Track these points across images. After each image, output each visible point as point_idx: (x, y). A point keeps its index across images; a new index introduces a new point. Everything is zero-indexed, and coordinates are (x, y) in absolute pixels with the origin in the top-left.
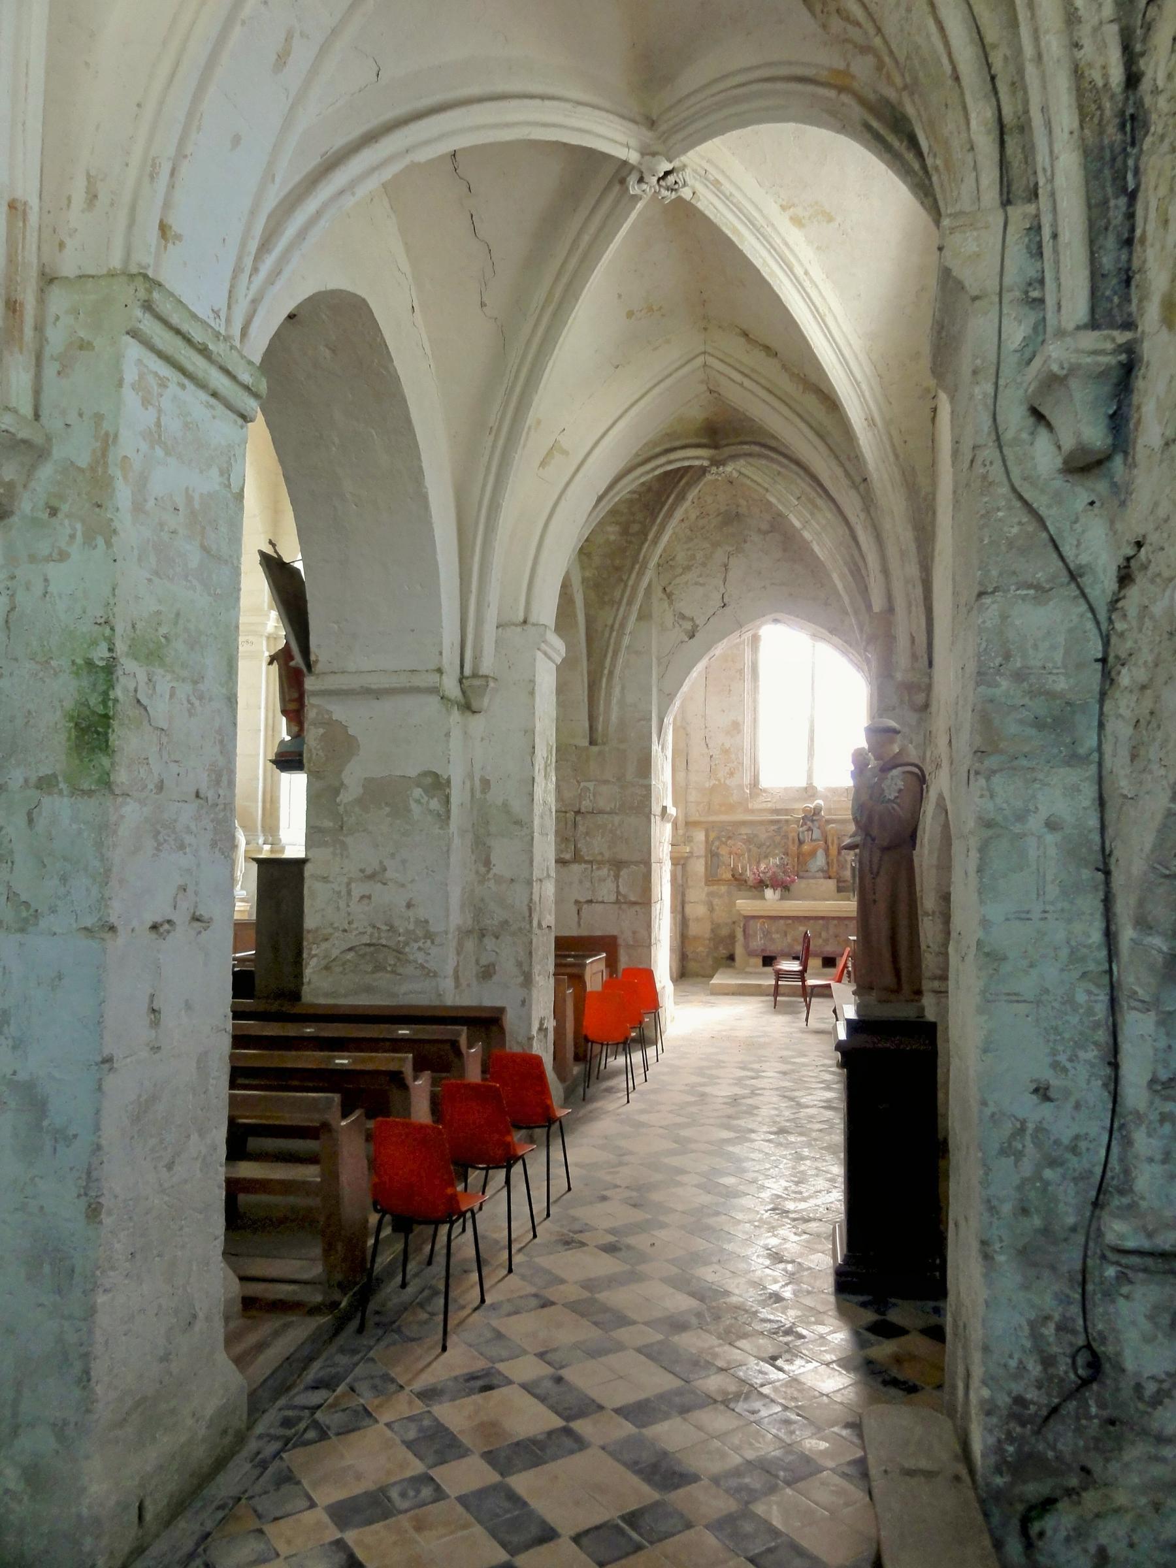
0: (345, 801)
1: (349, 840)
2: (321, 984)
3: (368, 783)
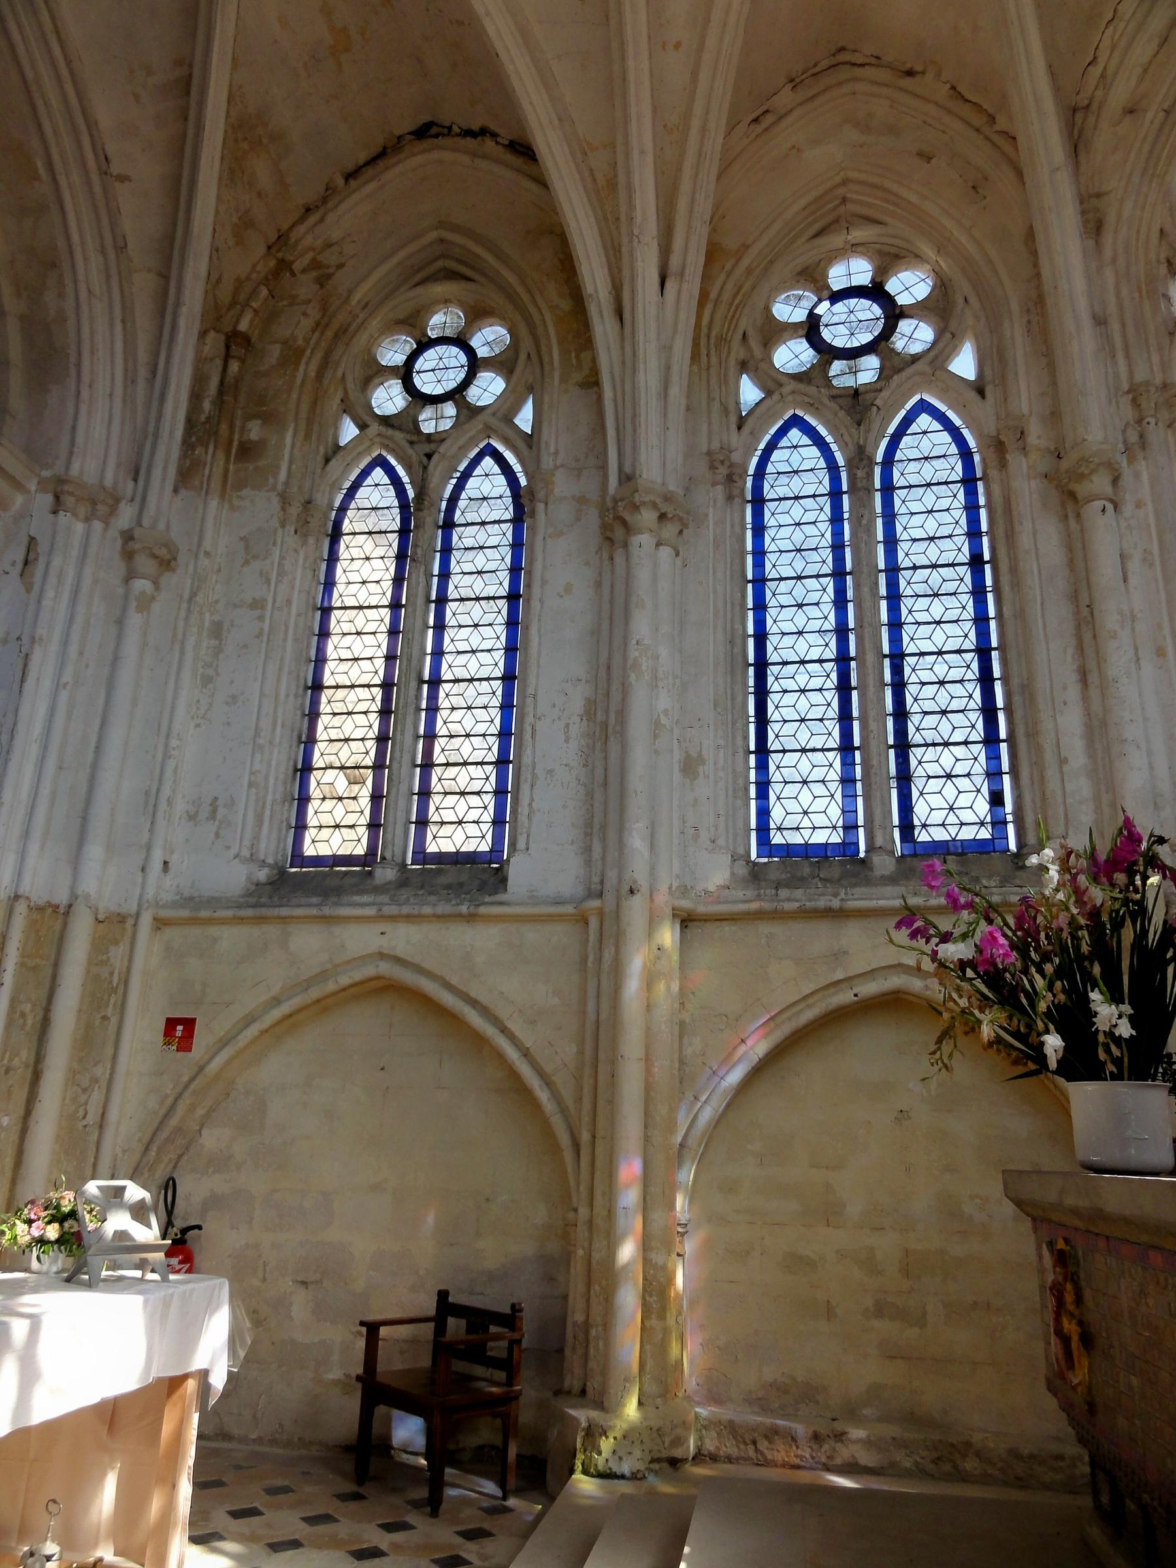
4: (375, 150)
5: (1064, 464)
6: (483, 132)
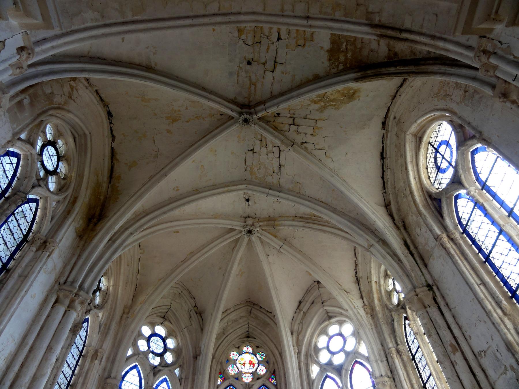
4: (104, 99)
5: (109, 381)
6: (113, 137)
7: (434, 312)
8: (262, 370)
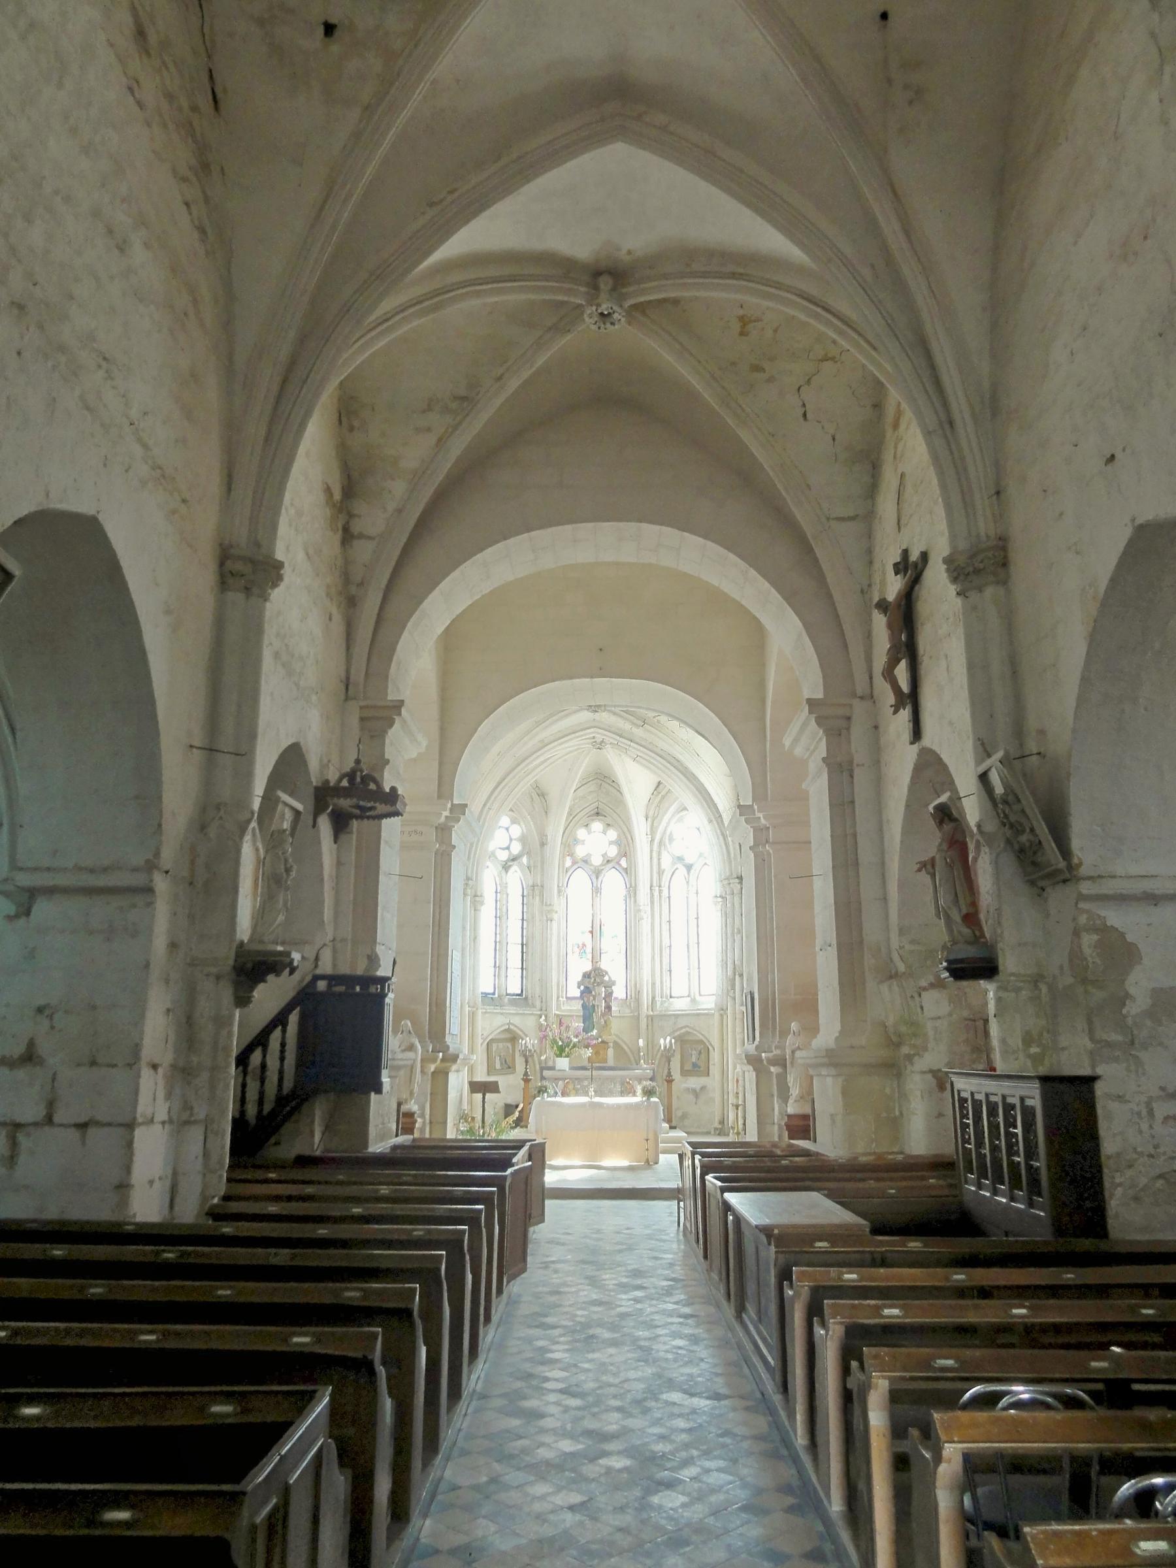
0: (1133, 1012)
1: (1144, 1055)
2: (1131, 1216)
3: (1156, 993)
7: (737, 899)
8: (613, 851)
